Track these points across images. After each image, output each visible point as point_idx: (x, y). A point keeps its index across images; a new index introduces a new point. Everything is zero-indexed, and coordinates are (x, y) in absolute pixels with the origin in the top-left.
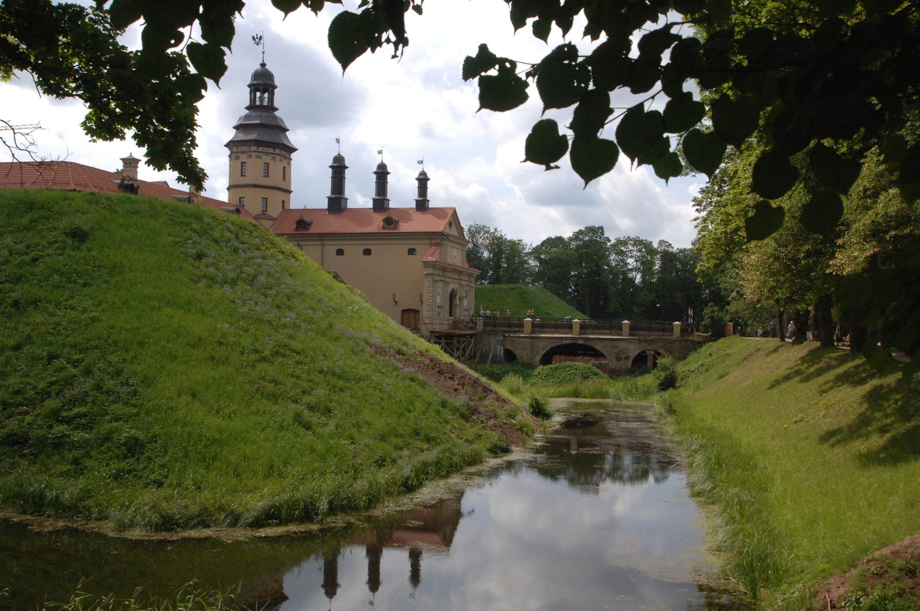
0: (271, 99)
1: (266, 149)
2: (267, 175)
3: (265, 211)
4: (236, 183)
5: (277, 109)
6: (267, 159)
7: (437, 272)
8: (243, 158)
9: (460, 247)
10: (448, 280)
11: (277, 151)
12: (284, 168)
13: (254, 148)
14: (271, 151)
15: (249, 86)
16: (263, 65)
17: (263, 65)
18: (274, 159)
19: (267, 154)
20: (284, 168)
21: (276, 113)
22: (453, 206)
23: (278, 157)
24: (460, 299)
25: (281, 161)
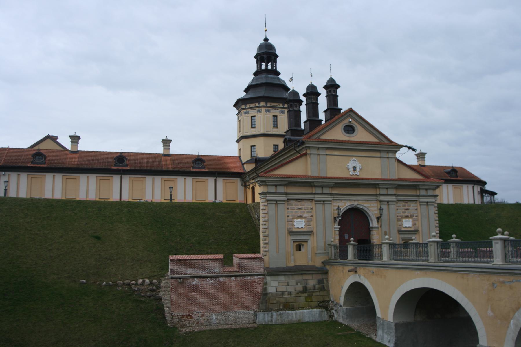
1: (252, 105)
6: (253, 113)
7: (281, 189)
9: (378, 155)
10: (318, 198)
11: (262, 104)
12: (275, 117)
13: (243, 107)
14: (257, 105)
16: (266, 40)
17: (266, 40)
18: (260, 111)
20: (277, 116)
22: (349, 108)
23: (263, 109)
24: (378, 219)
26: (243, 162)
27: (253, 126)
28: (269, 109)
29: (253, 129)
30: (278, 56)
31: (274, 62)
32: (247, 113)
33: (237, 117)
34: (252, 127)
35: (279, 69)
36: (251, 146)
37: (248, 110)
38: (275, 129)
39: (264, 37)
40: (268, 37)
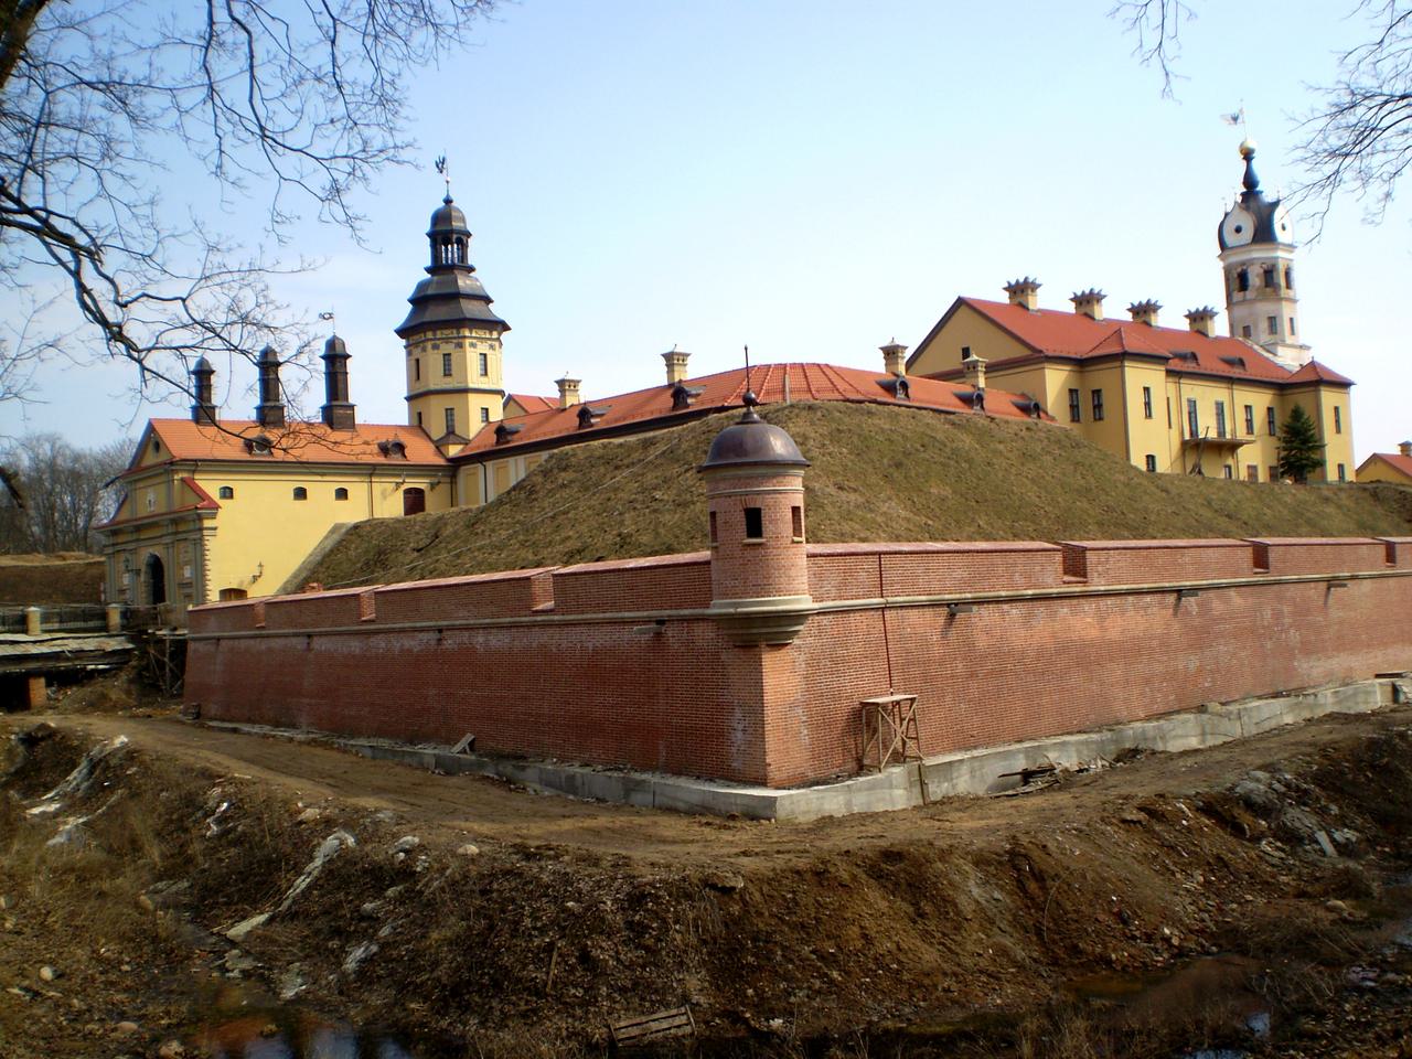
0: (463, 257)
1: (447, 332)
2: (447, 373)
3: (451, 432)
4: (413, 393)
5: (471, 269)
6: (446, 348)
8: (417, 352)
15: (429, 235)
16: (448, 201)
17: (448, 201)
19: (447, 340)
20: (485, 355)
21: (472, 274)
23: (467, 341)
25: (473, 345)
26: (435, 438)
27: (447, 373)
28: (474, 341)
29: (448, 379)
30: (469, 235)
31: (463, 245)
32: (436, 347)
33: (403, 352)
34: (445, 375)
35: (471, 261)
36: (447, 410)
37: (438, 342)
38: (484, 379)
39: (444, 196)
40: (453, 196)
